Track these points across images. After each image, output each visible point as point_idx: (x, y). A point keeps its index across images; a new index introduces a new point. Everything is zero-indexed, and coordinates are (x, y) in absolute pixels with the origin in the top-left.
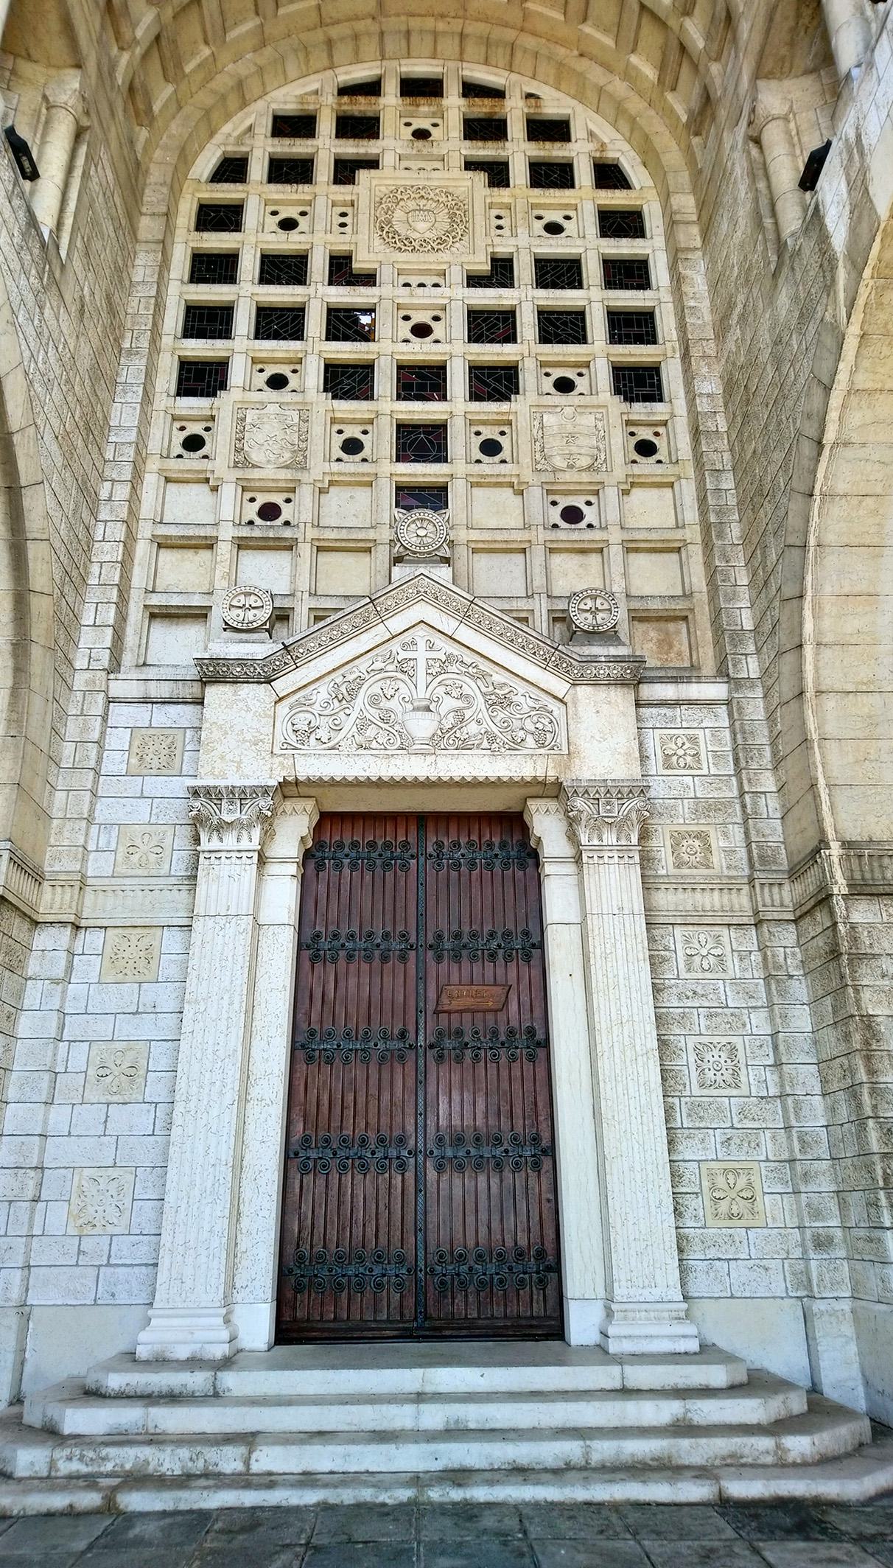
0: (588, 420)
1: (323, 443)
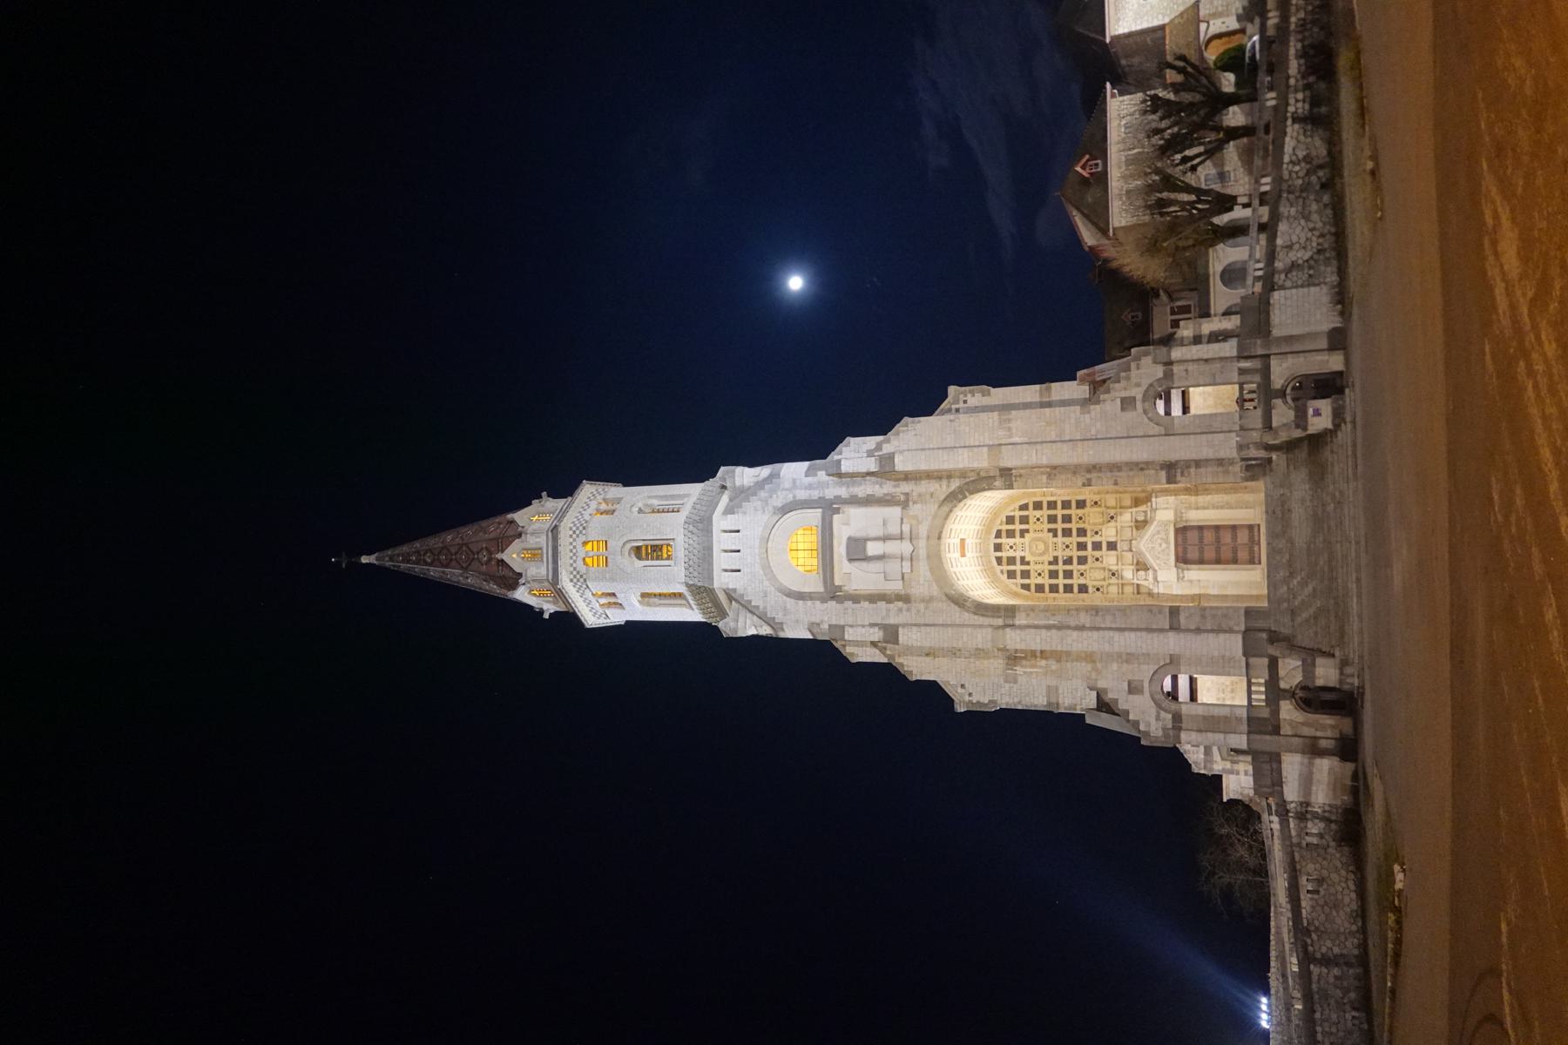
0: (1091, 515)
1: (1098, 564)
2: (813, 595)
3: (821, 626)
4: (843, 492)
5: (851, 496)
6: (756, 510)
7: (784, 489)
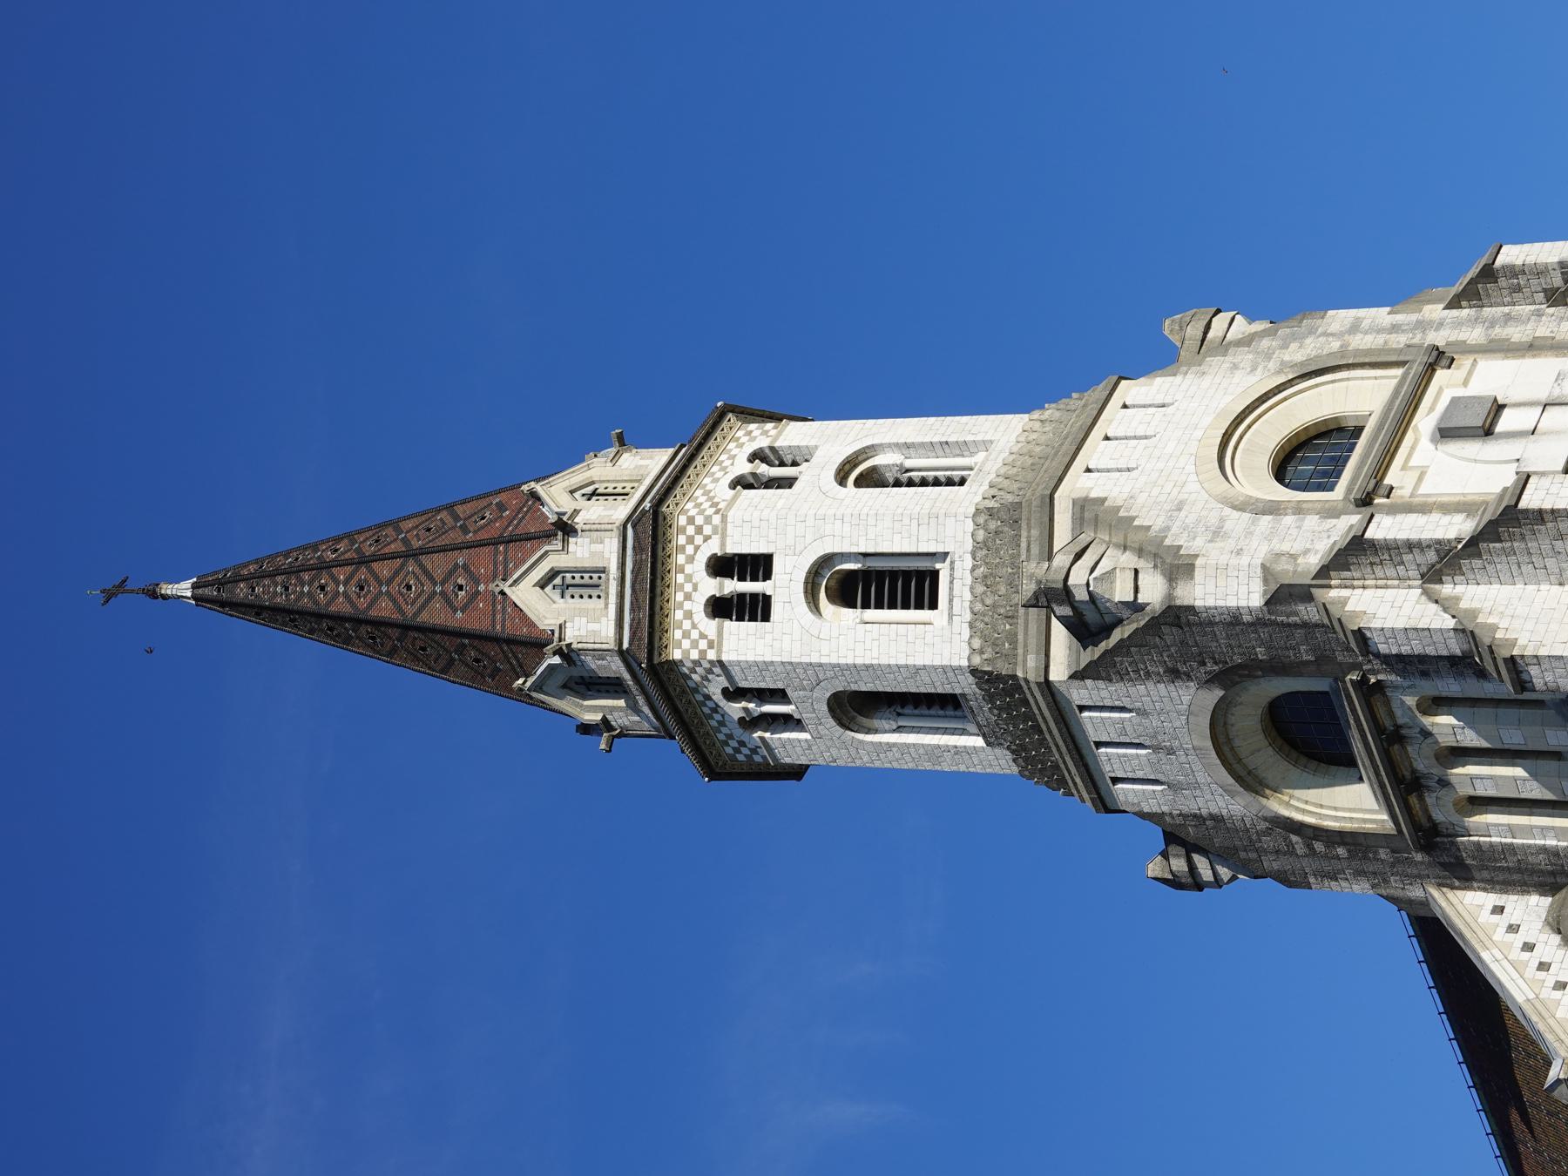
2: (1304, 506)
3: (1300, 560)
4: (1475, 335)
5: (1491, 341)
6: (1235, 367)
7: (1332, 335)
